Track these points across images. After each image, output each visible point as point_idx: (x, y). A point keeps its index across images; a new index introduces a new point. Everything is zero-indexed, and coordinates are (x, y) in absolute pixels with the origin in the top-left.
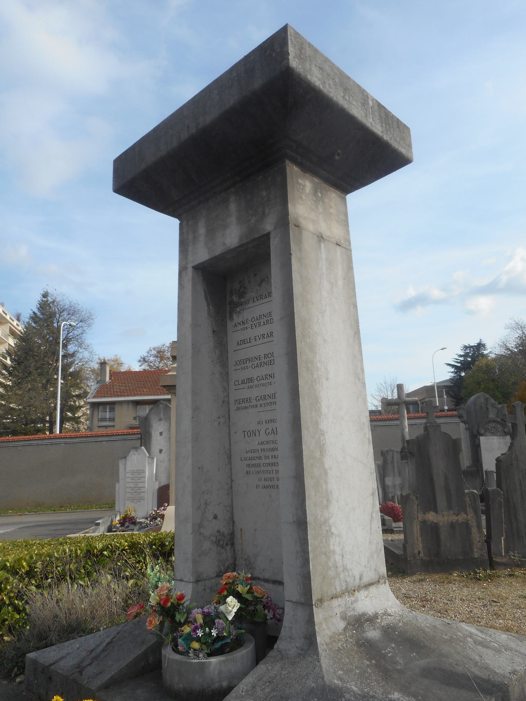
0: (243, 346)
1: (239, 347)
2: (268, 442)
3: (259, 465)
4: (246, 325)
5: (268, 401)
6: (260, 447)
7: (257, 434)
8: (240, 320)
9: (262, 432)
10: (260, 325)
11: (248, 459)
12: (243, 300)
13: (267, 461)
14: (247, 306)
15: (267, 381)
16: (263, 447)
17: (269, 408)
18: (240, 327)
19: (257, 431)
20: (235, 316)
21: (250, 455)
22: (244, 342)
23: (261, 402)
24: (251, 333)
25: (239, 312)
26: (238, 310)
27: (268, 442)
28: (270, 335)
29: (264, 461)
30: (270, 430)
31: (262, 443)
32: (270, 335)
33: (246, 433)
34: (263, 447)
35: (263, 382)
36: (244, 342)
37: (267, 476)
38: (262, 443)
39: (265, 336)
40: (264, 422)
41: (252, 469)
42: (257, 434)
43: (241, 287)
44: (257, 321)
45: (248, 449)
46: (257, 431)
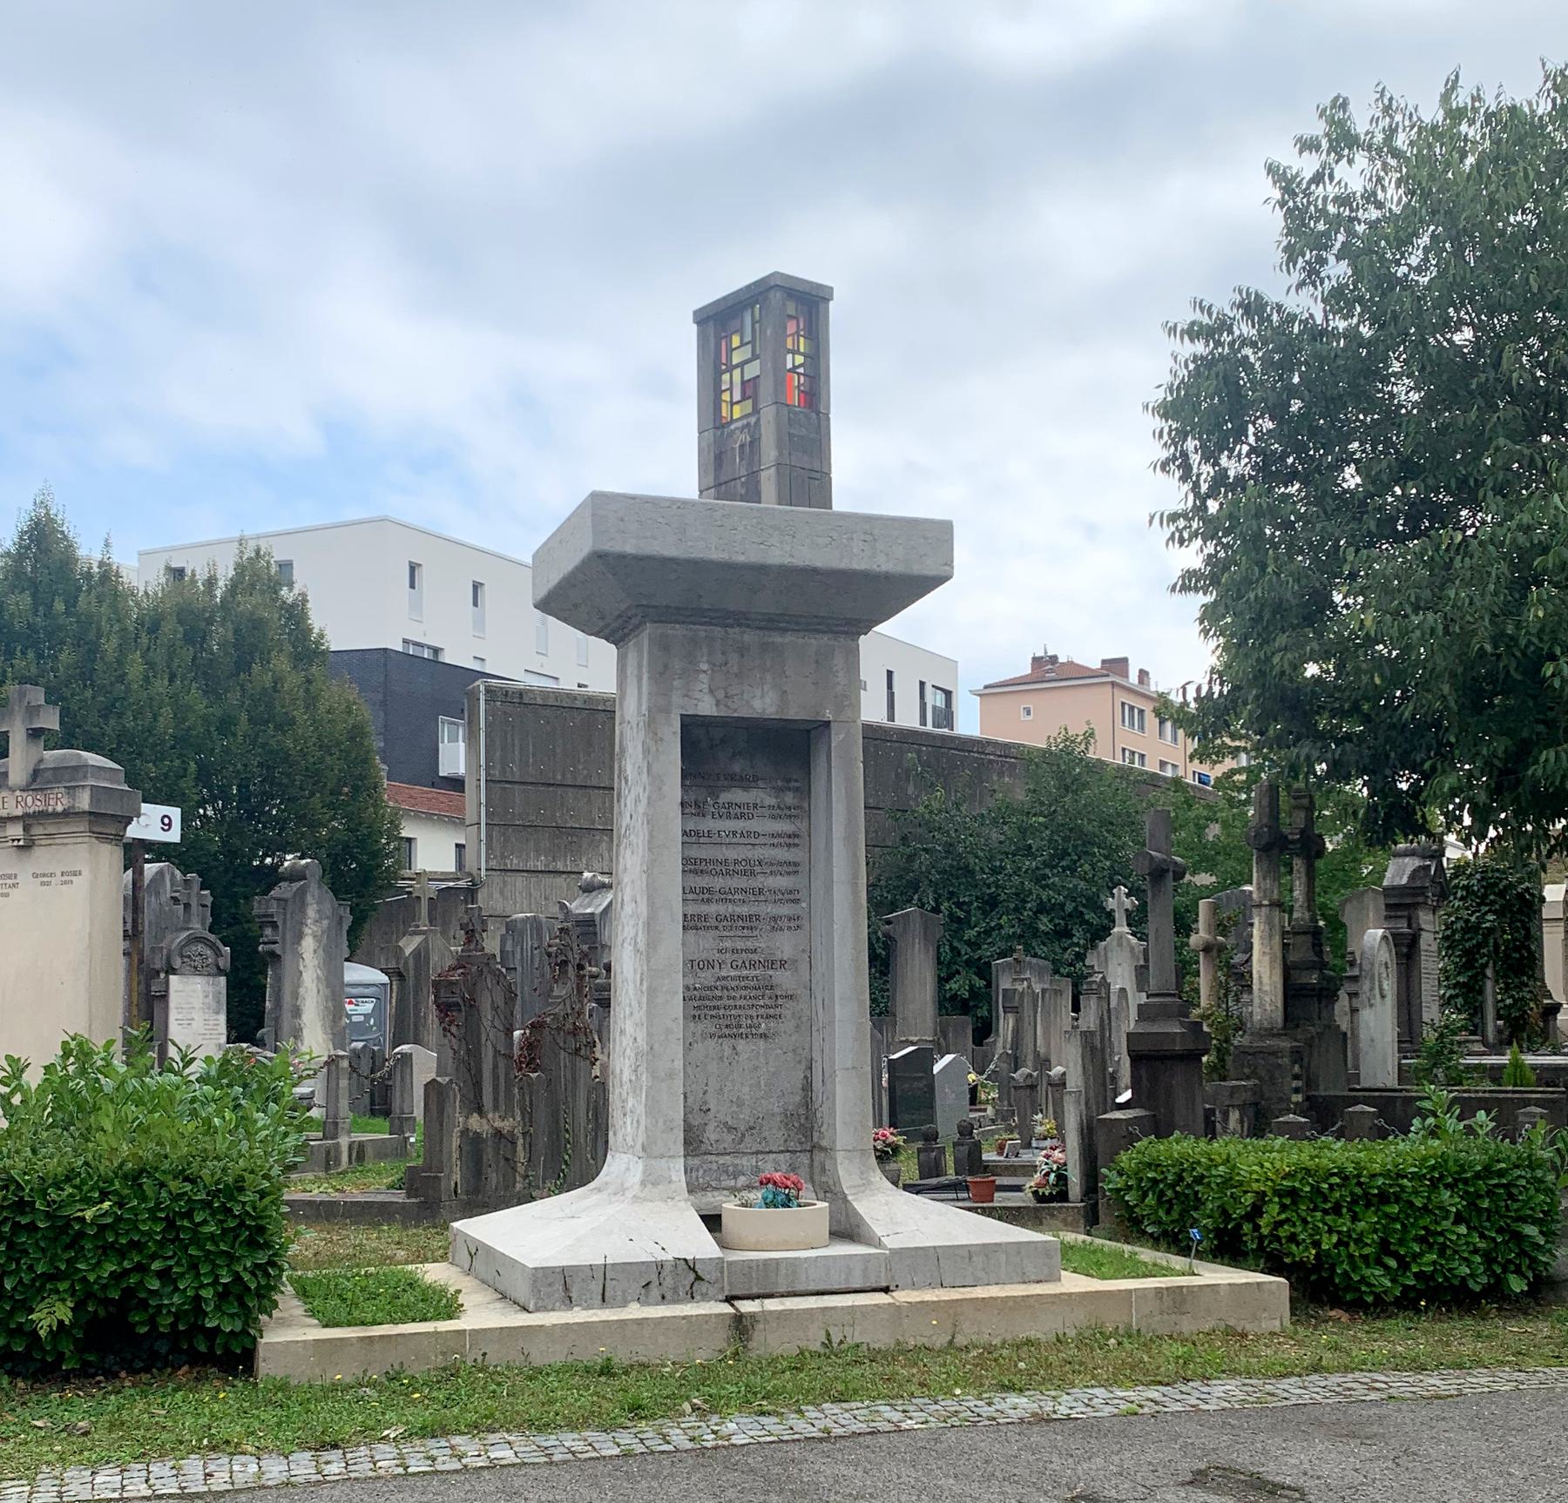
38: (725, 978)
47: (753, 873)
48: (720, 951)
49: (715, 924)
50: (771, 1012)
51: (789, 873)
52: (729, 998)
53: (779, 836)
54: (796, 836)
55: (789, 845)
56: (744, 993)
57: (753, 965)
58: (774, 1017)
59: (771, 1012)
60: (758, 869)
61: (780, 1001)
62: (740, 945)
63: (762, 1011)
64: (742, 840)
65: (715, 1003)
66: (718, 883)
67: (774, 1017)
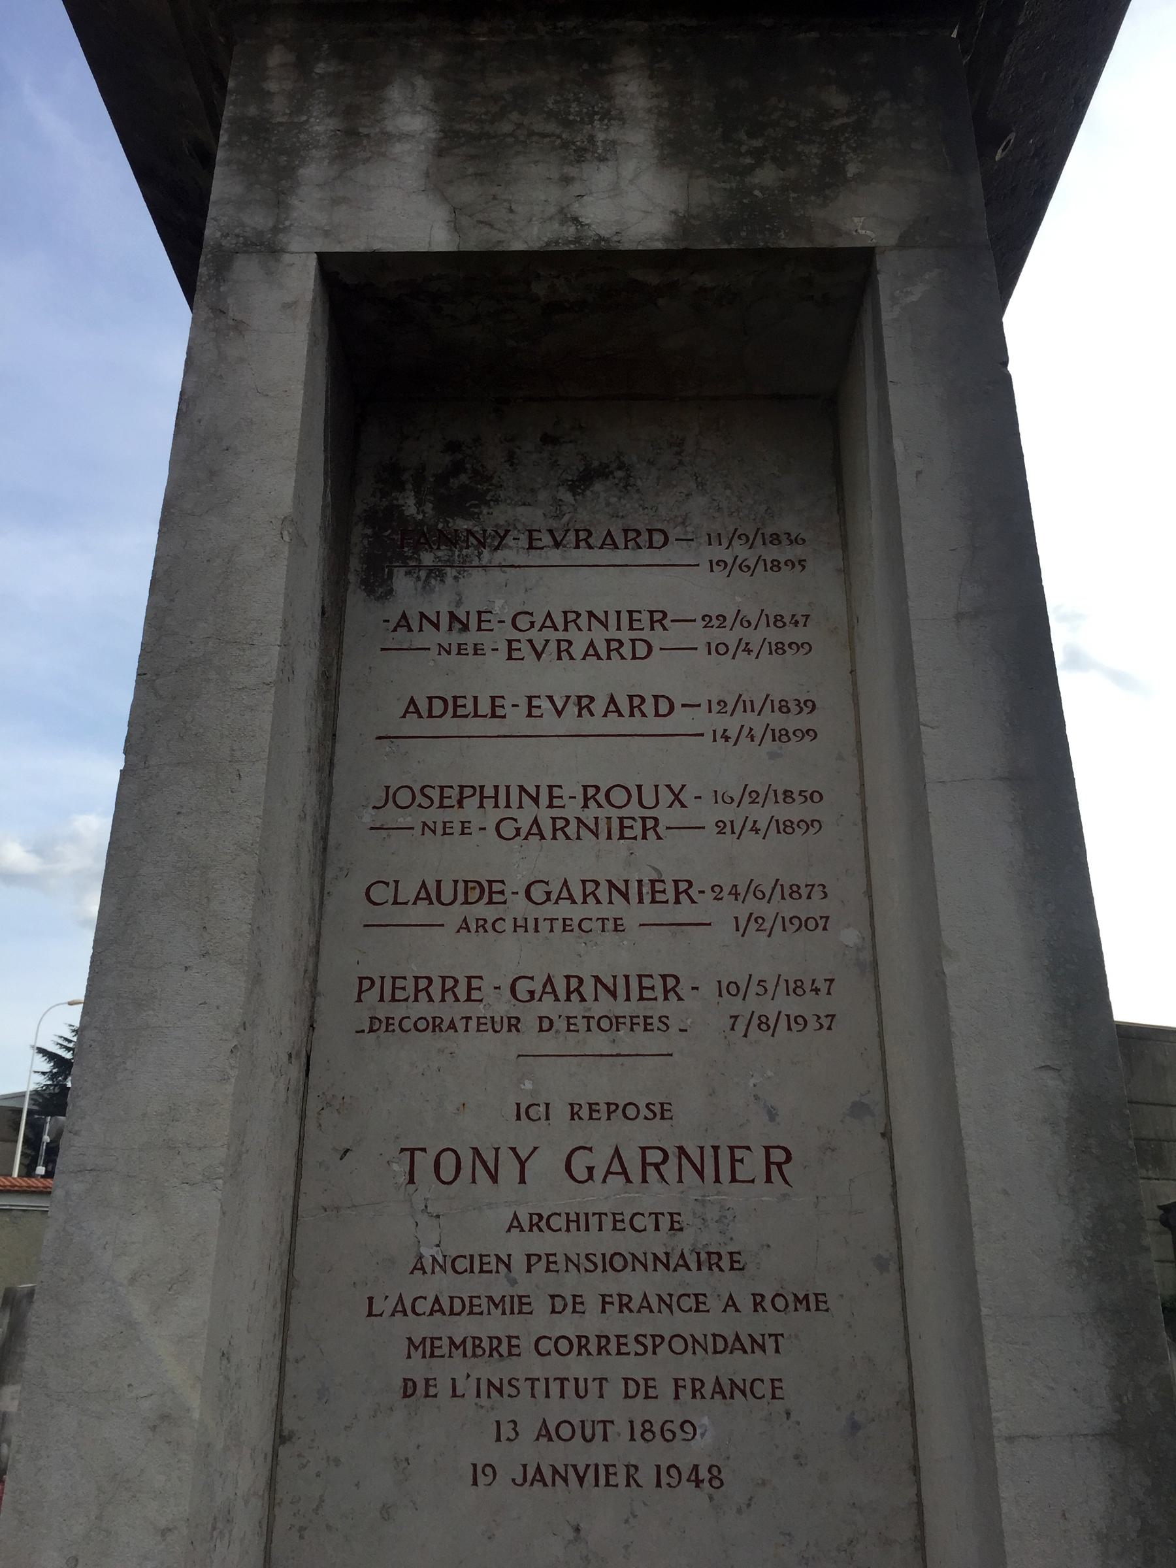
3: (502, 1348)
5: (598, 1010)
6: (518, 1246)
7: (509, 1169)
9: (545, 1165)
10: (564, 650)
11: (424, 1307)
16: (541, 1243)
19: (506, 1157)
21: (441, 1284)
22: (454, 706)
27: (576, 1222)
28: (625, 707)
30: (601, 1159)
31: (538, 1222)
32: (625, 707)
33: (424, 1162)
34: (541, 1243)
38: (538, 1222)
39: (599, 707)
40: (561, 1111)
42: (509, 1169)
44: (553, 635)
45: (427, 1252)
46: (506, 1157)
47: (650, 827)
48: (522, 1113)
49: (502, 1007)
50: (739, 1366)
56: (611, 1284)
57: (652, 1164)
58: (746, 1389)
59: (739, 1366)
60: (668, 816)
61: (770, 1321)
62: (601, 1085)
64: (613, 724)
65: (495, 1325)
66: (517, 864)
67: (746, 1389)
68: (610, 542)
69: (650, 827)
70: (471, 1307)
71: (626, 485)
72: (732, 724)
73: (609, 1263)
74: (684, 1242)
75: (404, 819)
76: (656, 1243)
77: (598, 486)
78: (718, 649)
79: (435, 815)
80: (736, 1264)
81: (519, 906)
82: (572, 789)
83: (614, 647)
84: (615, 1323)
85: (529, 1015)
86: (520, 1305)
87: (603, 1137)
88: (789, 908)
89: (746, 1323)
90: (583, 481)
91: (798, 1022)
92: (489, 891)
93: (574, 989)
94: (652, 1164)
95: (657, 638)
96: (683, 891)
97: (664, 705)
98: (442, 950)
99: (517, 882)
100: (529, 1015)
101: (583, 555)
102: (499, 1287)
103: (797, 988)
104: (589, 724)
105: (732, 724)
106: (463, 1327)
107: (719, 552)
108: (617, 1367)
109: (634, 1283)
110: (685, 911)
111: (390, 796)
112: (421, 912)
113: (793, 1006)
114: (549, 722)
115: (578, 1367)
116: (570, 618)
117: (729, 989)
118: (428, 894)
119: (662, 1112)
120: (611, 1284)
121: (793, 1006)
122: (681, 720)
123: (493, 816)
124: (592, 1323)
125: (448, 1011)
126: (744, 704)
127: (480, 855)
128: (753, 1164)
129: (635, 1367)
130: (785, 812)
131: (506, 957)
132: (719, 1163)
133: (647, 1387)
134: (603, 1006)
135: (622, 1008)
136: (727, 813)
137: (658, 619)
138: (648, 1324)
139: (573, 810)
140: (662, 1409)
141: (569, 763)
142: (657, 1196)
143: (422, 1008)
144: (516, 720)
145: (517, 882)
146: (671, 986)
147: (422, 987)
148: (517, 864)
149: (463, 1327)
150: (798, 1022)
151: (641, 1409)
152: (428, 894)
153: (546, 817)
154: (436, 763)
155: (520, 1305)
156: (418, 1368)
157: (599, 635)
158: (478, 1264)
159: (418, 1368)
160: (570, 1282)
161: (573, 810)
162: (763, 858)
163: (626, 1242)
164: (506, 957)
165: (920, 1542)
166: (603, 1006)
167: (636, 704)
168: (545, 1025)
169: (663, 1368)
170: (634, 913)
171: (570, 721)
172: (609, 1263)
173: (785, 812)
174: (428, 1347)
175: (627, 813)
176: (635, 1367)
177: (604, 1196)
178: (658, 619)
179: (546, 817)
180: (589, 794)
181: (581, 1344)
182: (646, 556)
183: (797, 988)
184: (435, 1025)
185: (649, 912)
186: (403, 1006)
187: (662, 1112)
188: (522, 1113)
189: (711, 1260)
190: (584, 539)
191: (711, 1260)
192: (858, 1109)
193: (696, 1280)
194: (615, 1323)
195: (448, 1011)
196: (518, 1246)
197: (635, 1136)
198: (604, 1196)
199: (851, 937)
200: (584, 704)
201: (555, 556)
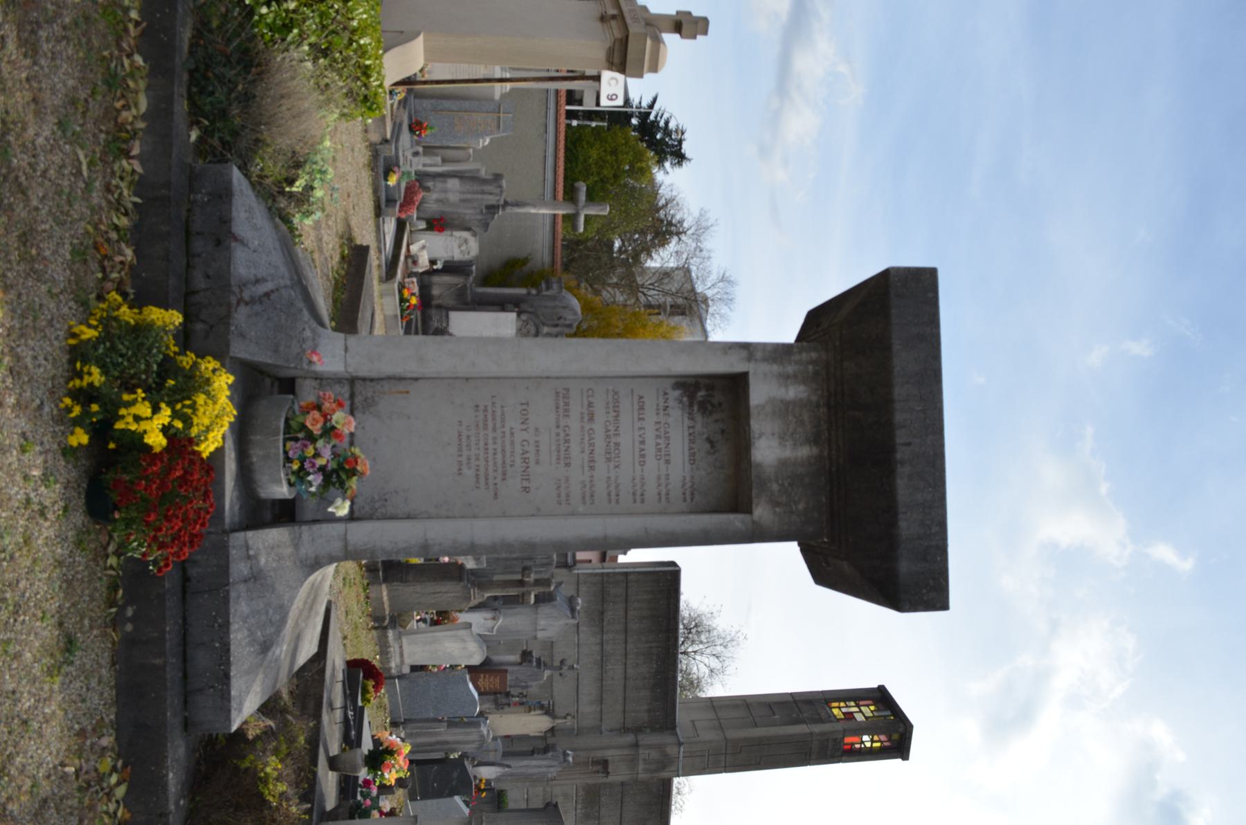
0: (636, 407)
1: (636, 398)
2: (512, 443)
3: (486, 427)
4: (662, 412)
6: (507, 430)
7: (524, 427)
8: (671, 403)
9: (525, 435)
10: (658, 437)
12: (696, 408)
13: (490, 441)
14: (686, 419)
15: (587, 445)
16: (508, 435)
17: (554, 447)
18: (661, 400)
20: (677, 393)
21: (498, 413)
22: (641, 408)
23: (562, 434)
24: (651, 417)
25: (681, 402)
26: (685, 399)
27: (512, 443)
29: (491, 435)
30: (526, 448)
31: (512, 434)
34: (508, 435)
35: (587, 438)
36: (641, 408)
37: (473, 439)
38: (512, 434)
41: (481, 417)
42: (524, 427)
43: (713, 406)
47: (609, 460)
48: (537, 430)
49: (562, 424)
50: (482, 480)
51: (609, 494)
52: (495, 438)
53: (643, 485)
54: (643, 501)
55: (634, 494)
57: (525, 460)
58: (478, 482)
59: (482, 480)
60: (612, 464)
61: (492, 487)
63: (482, 473)
64: (637, 450)
65: (490, 424)
66: (598, 426)
67: (478, 482)
68: (691, 449)
69: (609, 460)
70: (494, 419)
71: (709, 453)
72: (637, 481)
73: (503, 450)
74: (508, 468)
75: (610, 399)
76: (508, 461)
77: (708, 445)
78: (659, 478)
79: (611, 405)
80: (504, 479)
81: (587, 427)
82: (619, 440)
83: (659, 450)
84: (491, 451)
85: (560, 430)
86: (494, 430)
87: (532, 449)
88: (588, 495)
89: (491, 482)
90: (709, 440)
91: (559, 496)
92: (591, 418)
93: (567, 441)
94: (525, 460)
95: (662, 462)
96: (592, 468)
97: (642, 464)
98: (576, 409)
99: (593, 426)
100: (560, 430)
101: (687, 441)
102: (498, 425)
103: (568, 495)
104: (637, 443)
105: (637, 481)
106: (490, 417)
107: (688, 479)
108: (482, 453)
109: (499, 456)
110: (586, 468)
111: (616, 393)
112: (586, 403)
113: (563, 495)
114: (637, 433)
115: (482, 444)
116: (668, 438)
117: (567, 479)
118: (590, 404)
119: (537, 462)
120: (499, 450)
121: (563, 495)
122: (638, 467)
123: (611, 419)
124: (491, 447)
125: (561, 411)
126: (643, 485)
127: (601, 416)
128: (525, 484)
129: (482, 456)
130: (613, 494)
131: (574, 424)
132: (526, 476)
133: (478, 459)
134: (563, 448)
135: (562, 453)
136: (613, 479)
137: (668, 462)
138: (490, 458)
139: (613, 440)
140: (473, 462)
141: (626, 439)
142: (518, 461)
143: (562, 404)
144: (638, 424)
145: (593, 426)
146: (568, 465)
147: (567, 404)
148: (598, 426)
149: (490, 417)
150: (559, 496)
151: (473, 458)
152: (590, 404)
153: (611, 433)
154: (626, 405)
155: (494, 430)
156: (481, 408)
157: (663, 446)
158: (503, 420)
159: (481, 408)
160: (499, 441)
161: (613, 440)
162: (600, 488)
163: (508, 454)
164: (574, 424)
165: (448, 517)
166: (563, 448)
167: (643, 456)
168: (558, 434)
169: (482, 463)
170: (586, 457)
171: (637, 439)
172: (503, 450)
173: (613, 494)
174: (486, 410)
175: (612, 452)
176: (482, 456)
177: (518, 450)
178: (668, 462)
179: (611, 433)
180: (617, 444)
181: (486, 444)
182: (687, 459)
183: (568, 495)
184: (557, 408)
185: (586, 459)
186: (562, 399)
187: (537, 462)
188: (537, 430)
189: (504, 474)
190: (692, 441)
191: (504, 474)
192: (539, 509)
193: (500, 470)
194: (491, 451)
195: (561, 411)
196: (507, 430)
197: (532, 456)
198: (518, 450)
199: (581, 509)
200: (642, 442)
201: (686, 434)
